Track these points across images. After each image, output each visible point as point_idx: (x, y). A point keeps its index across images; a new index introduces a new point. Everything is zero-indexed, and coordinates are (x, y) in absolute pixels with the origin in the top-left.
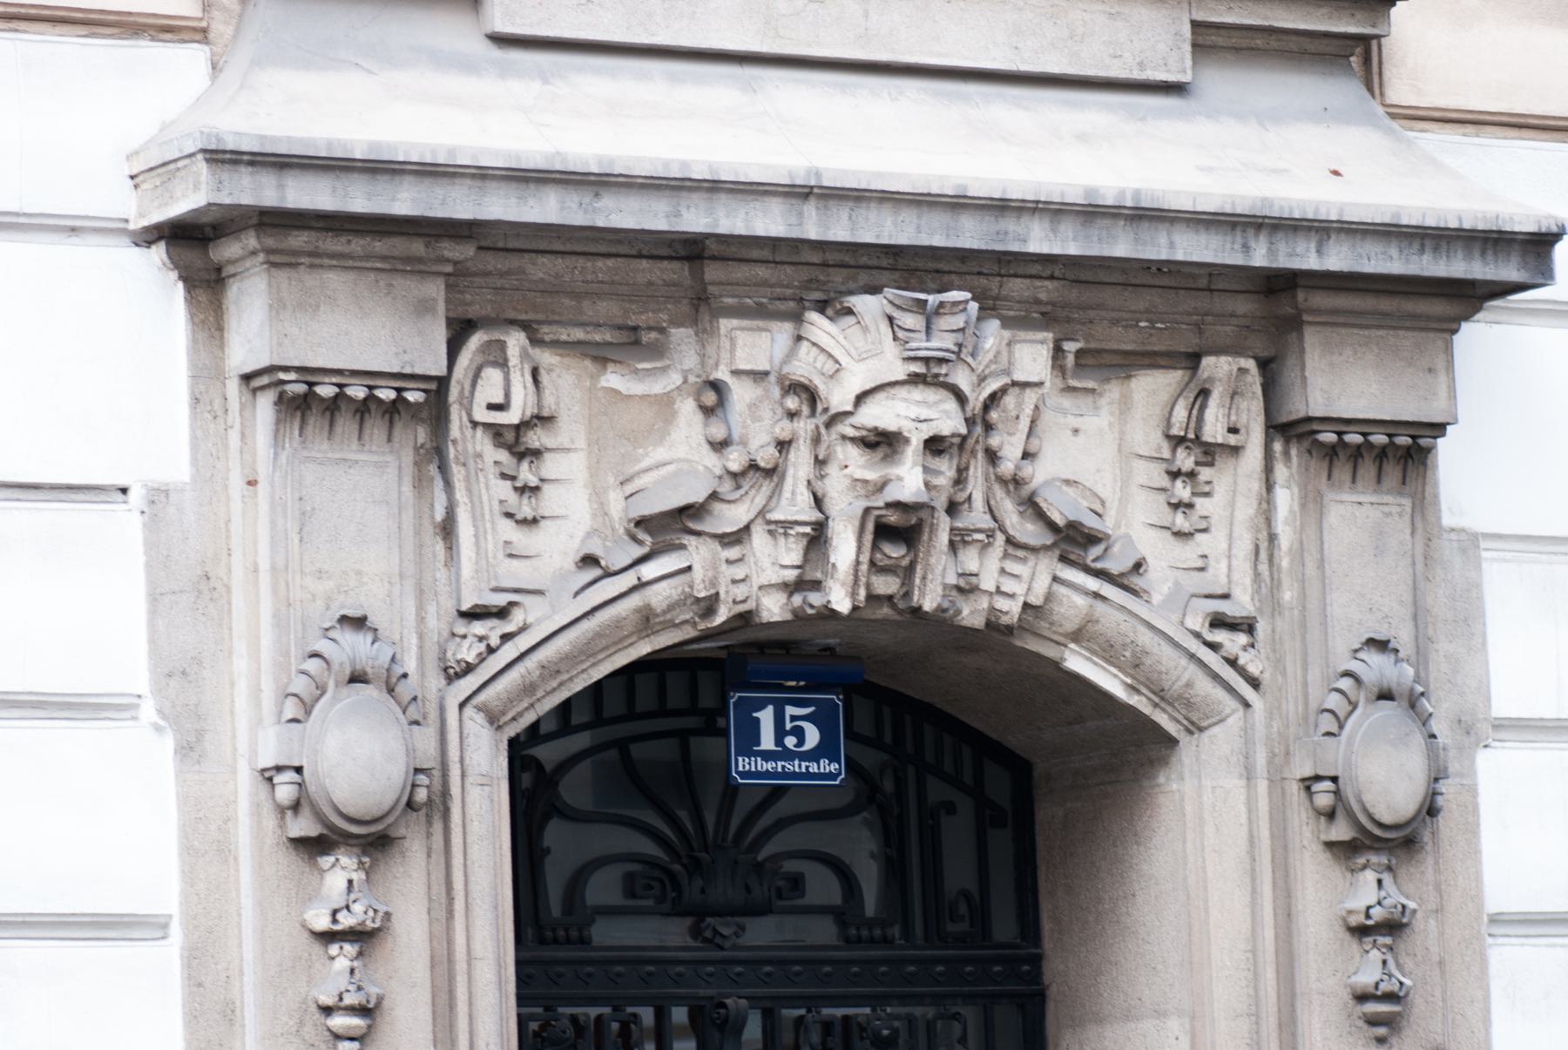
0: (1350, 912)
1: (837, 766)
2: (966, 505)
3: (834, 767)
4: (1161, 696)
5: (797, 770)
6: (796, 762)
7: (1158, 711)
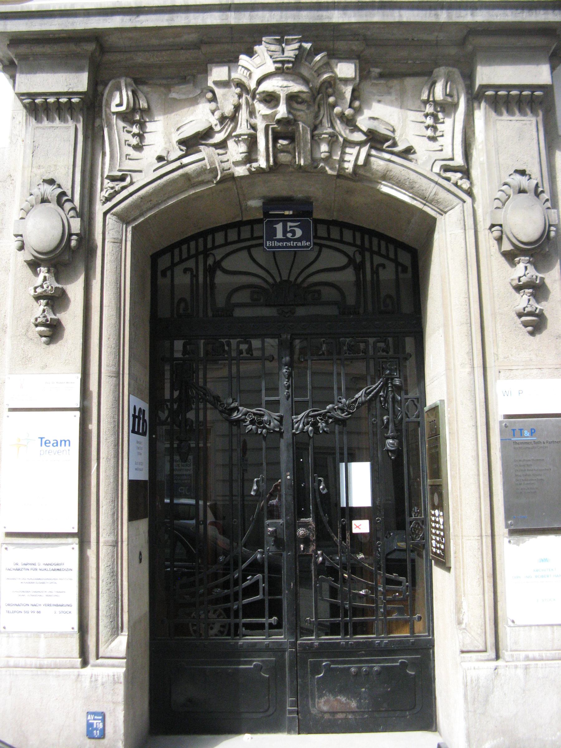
0: (512, 280)
1: (309, 243)
2: (320, 125)
3: (308, 244)
4: (425, 199)
5: (292, 245)
6: (292, 242)
7: (425, 207)
